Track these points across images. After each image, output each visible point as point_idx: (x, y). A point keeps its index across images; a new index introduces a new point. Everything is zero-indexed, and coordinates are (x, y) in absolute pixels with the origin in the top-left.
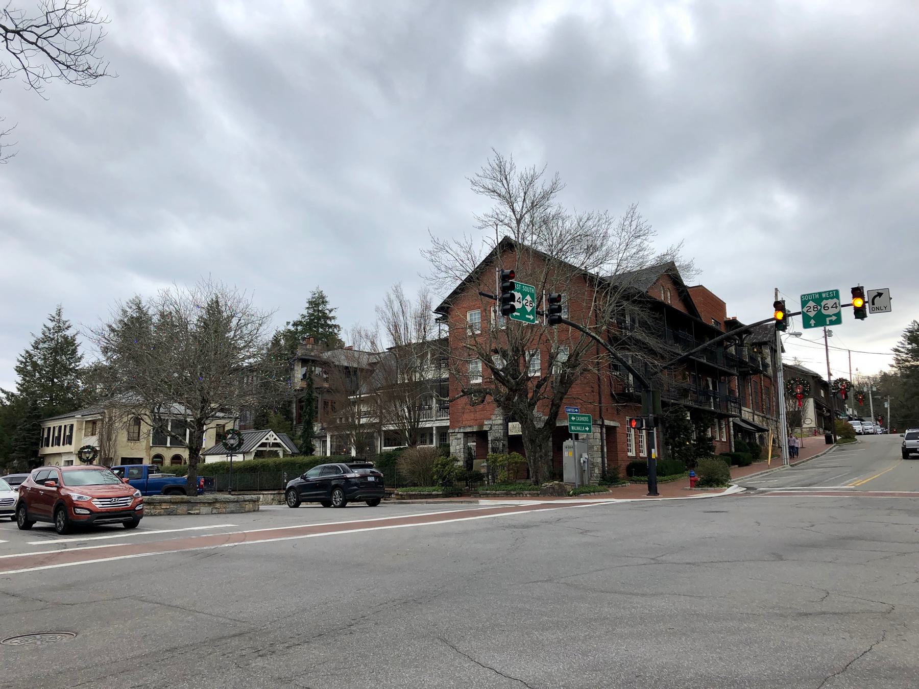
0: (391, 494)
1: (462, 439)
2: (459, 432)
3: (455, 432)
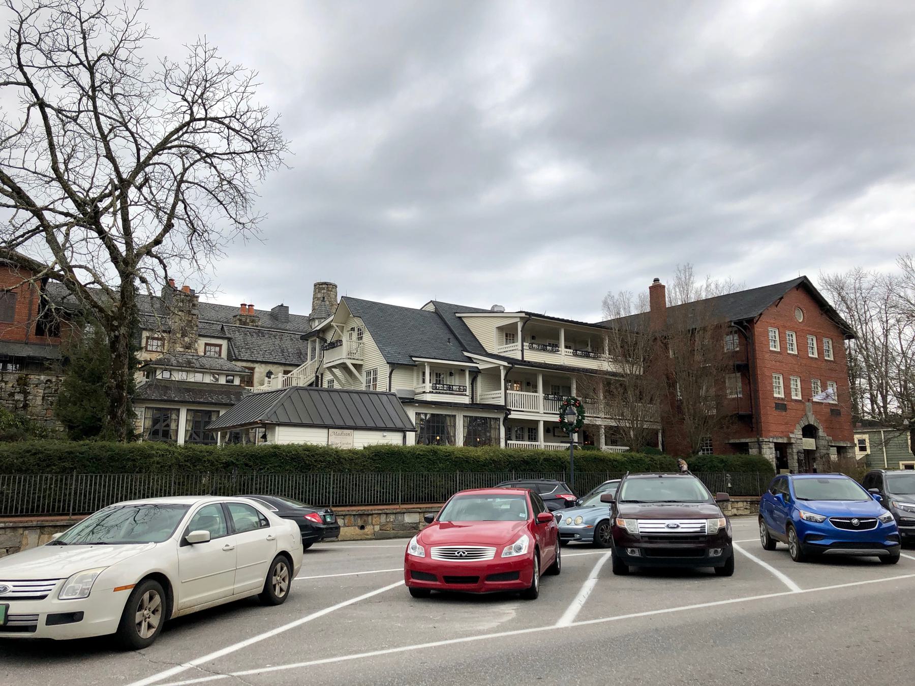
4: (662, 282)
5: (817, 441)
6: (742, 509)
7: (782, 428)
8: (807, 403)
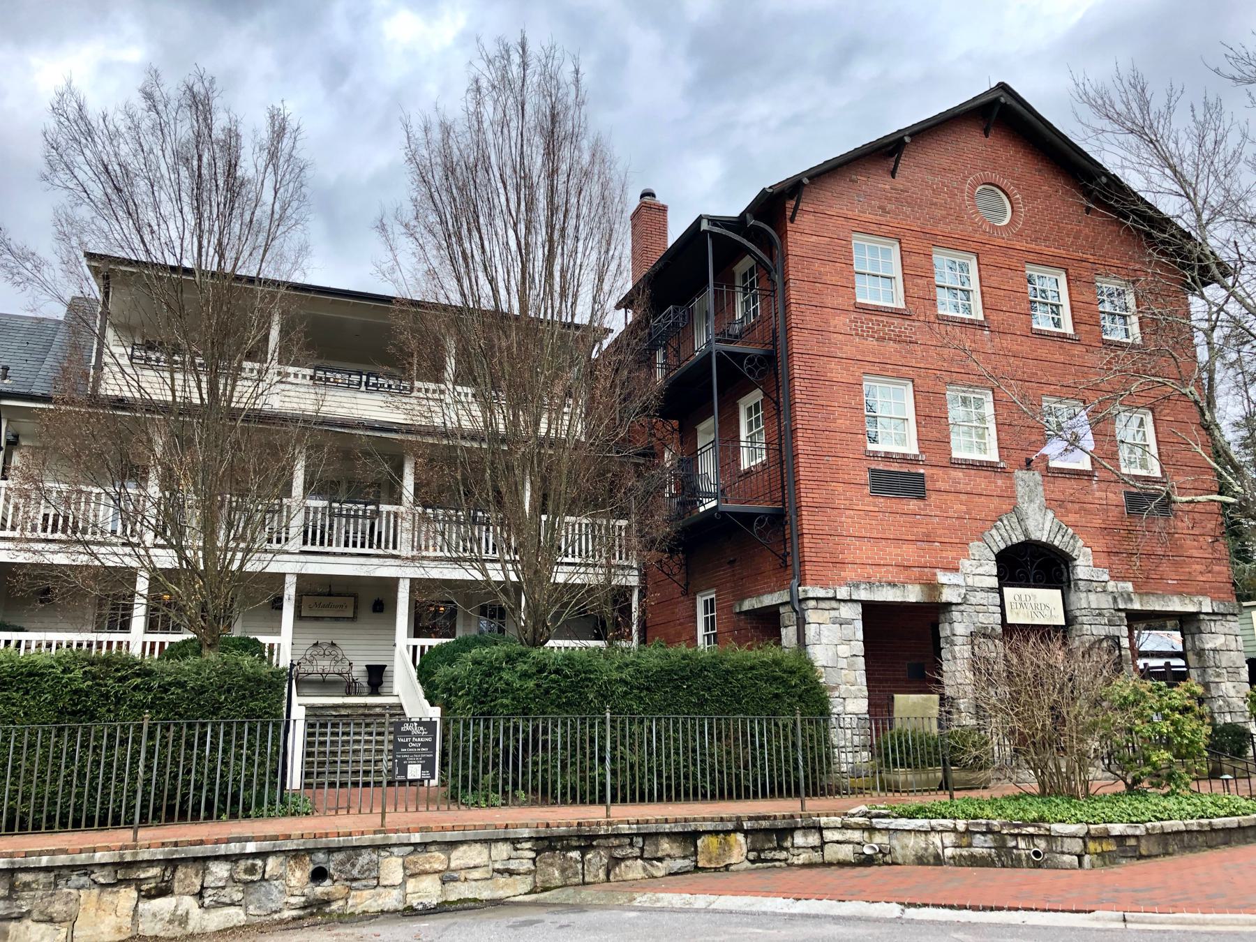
0: (781, 833)
1: (859, 625)
2: (851, 601)
3: (834, 599)
4: (661, 199)
5: (1073, 597)
6: (476, 874)
7: (909, 553)
8: (1019, 474)
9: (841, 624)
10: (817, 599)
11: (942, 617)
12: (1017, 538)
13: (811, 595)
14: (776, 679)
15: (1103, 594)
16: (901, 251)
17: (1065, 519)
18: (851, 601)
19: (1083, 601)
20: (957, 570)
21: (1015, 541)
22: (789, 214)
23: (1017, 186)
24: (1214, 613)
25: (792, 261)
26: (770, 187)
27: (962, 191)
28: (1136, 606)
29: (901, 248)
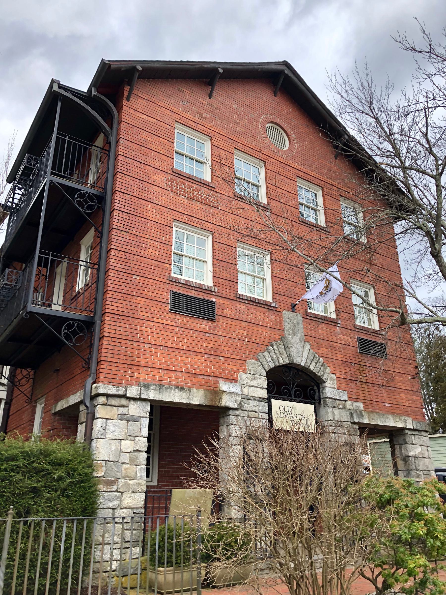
1: (146, 422)
2: (141, 399)
3: (124, 396)
5: (322, 411)
8: (288, 314)
9: (128, 421)
10: (108, 396)
11: (222, 421)
12: (283, 360)
13: (101, 391)
14: (38, 471)
15: (343, 410)
16: (212, 145)
17: (318, 351)
18: (141, 399)
19: (330, 414)
20: (236, 381)
21: (282, 362)
22: (126, 94)
23: (293, 130)
24: (414, 430)
25: (123, 125)
26: (109, 61)
27: (257, 122)
28: (366, 421)
29: (212, 143)
